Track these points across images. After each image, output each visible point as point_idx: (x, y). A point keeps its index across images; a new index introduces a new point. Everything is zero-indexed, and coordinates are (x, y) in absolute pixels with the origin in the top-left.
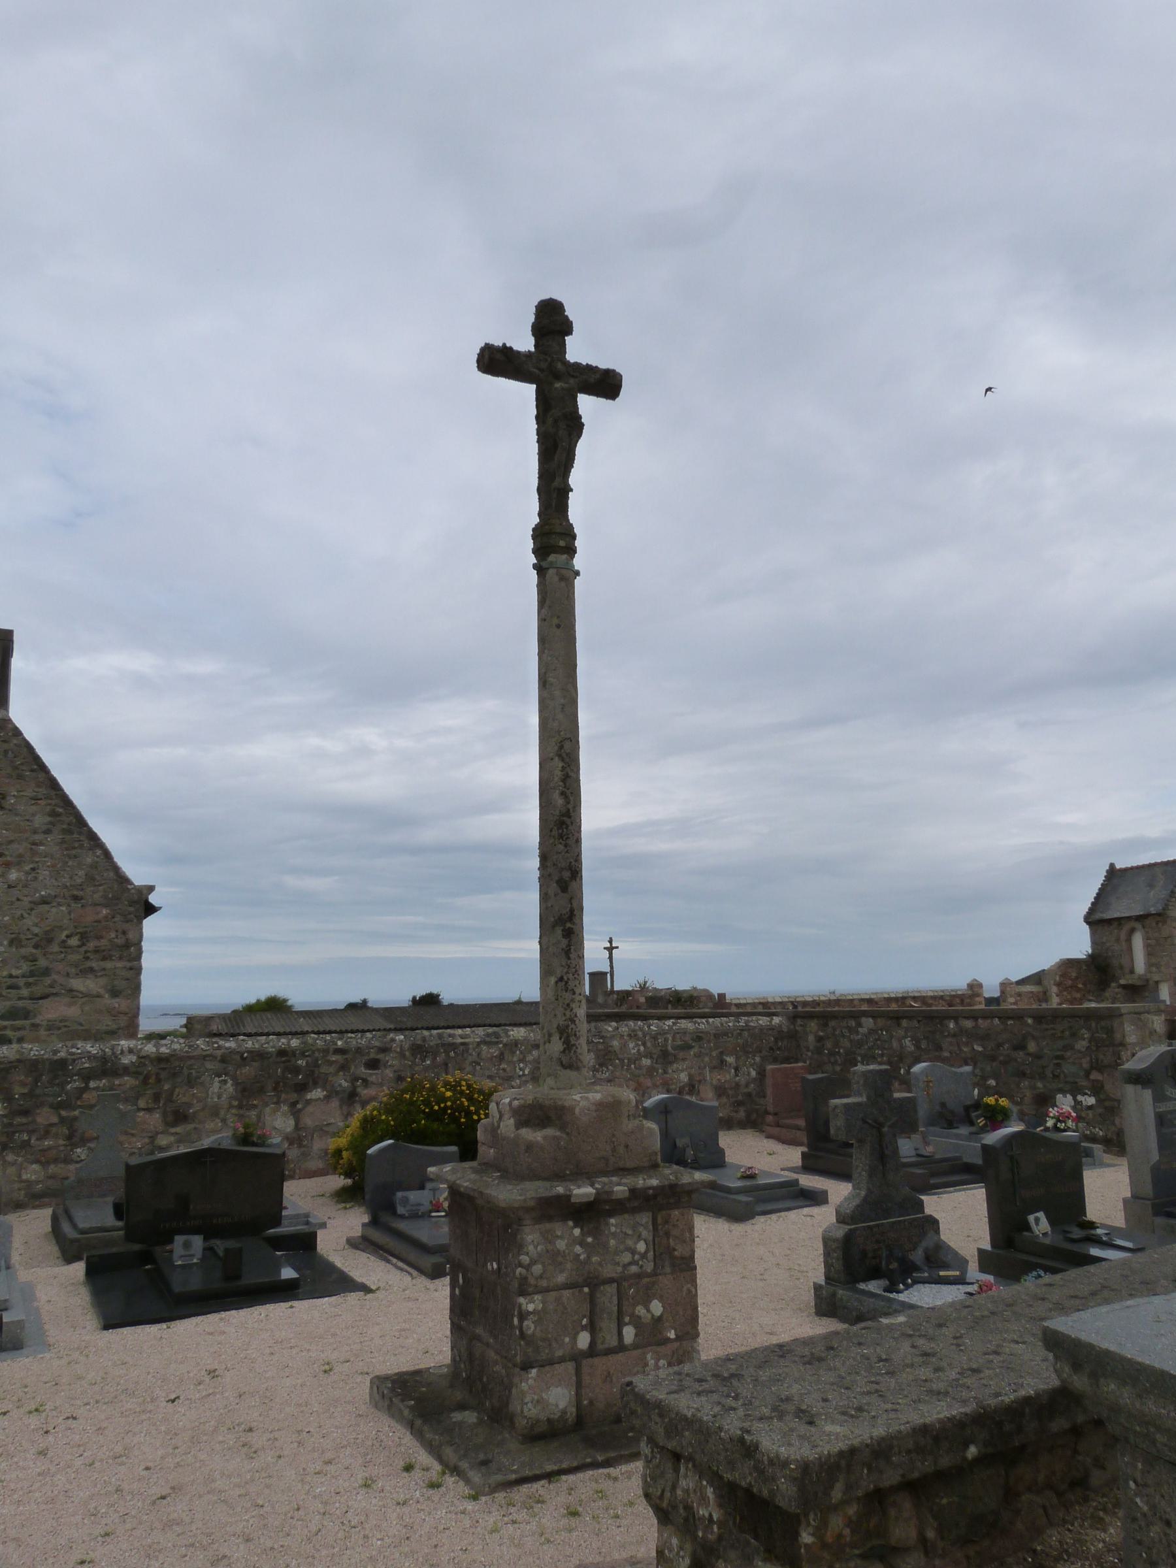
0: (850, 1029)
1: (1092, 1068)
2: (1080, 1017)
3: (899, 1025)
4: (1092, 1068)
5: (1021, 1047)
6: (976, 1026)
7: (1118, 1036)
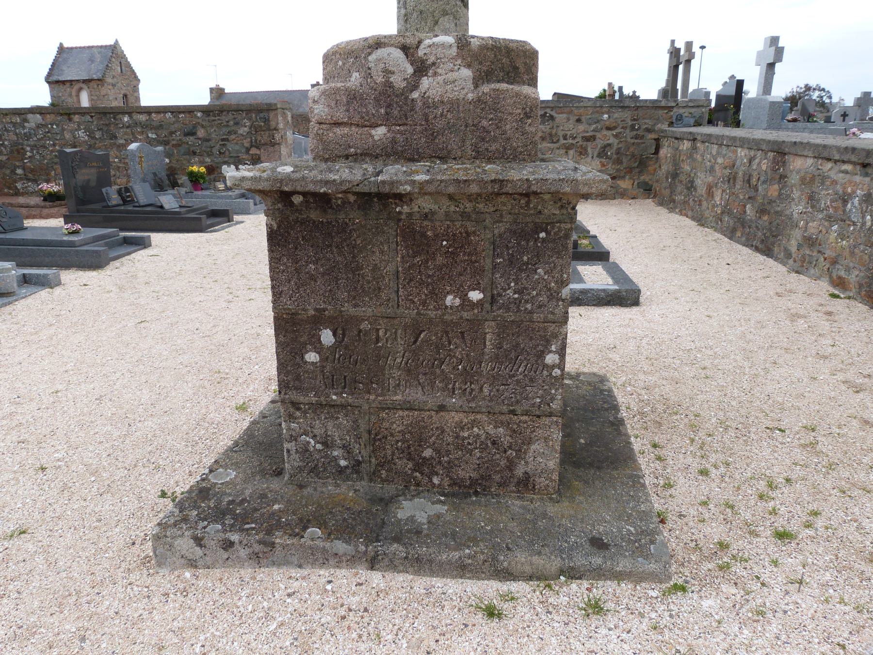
0: (14, 124)
1: (252, 146)
2: (242, 111)
3: (70, 120)
4: (252, 146)
5: (192, 133)
6: (151, 120)
7: (273, 124)
